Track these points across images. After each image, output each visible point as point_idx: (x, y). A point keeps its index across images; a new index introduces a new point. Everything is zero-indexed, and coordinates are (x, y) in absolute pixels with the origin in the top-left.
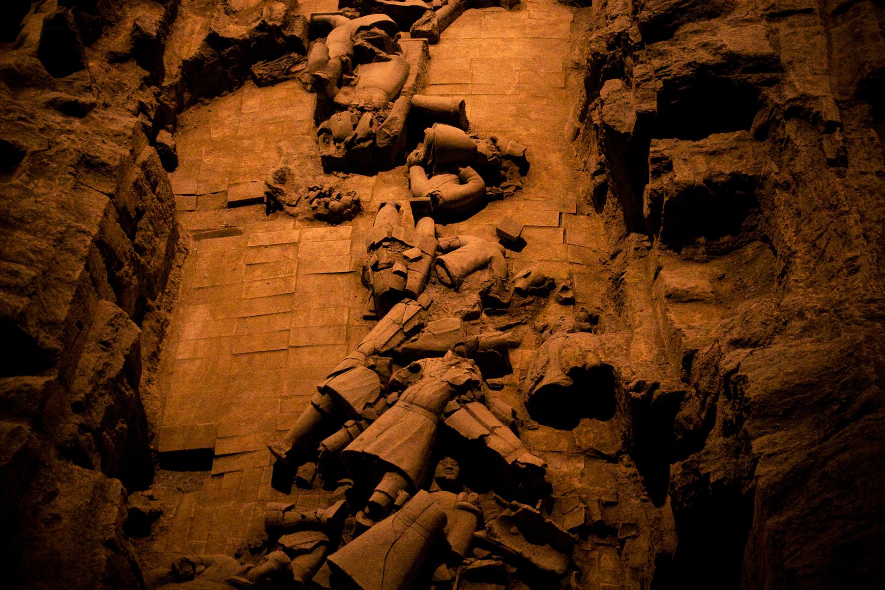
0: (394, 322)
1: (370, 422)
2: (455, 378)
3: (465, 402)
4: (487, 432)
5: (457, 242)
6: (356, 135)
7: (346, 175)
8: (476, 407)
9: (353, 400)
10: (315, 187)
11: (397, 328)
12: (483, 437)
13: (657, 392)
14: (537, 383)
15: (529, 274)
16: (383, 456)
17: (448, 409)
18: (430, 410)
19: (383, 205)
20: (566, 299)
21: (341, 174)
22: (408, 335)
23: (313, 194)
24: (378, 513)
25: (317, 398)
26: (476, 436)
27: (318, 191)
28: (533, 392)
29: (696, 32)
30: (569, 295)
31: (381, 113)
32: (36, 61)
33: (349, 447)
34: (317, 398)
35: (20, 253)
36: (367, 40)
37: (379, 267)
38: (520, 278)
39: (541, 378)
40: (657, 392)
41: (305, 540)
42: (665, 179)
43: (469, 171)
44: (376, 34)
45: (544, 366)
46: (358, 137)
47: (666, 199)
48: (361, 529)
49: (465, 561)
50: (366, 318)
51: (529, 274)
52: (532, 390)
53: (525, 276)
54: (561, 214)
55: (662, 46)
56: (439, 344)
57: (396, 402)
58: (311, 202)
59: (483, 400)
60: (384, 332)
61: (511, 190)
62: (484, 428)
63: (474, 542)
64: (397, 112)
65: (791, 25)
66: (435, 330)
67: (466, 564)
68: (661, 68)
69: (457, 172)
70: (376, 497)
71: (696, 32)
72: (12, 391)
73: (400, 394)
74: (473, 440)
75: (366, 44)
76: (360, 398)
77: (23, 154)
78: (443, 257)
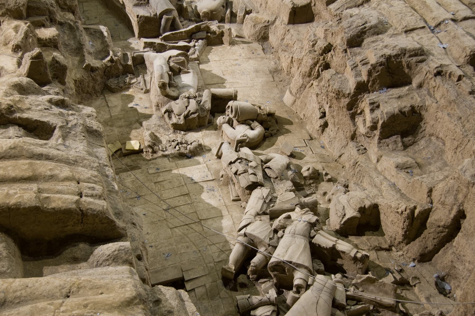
0: (259, 198)
1: (275, 247)
2: (310, 219)
3: (317, 230)
4: (335, 243)
5: (269, 158)
6: (190, 111)
7: (185, 133)
8: (321, 232)
9: (263, 237)
10: (174, 140)
11: (262, 201)
12: (334, 246)
13: (417, 212)
14: (343, 218)
15: (309, 169)
16: (294, 261)
17: (312, 235)
18: (304, 236)
19: (222, 144)
20: (329, 179)
21: (183, 132)
22: (268, 204)
23: (174, 144)
24: (299, 289)
25: (241, 239)
26: (331, 246)
27: (176, 142)
28: (342, 223)
29: (373, 42)
30: (329, 177)
31: (198, 99)
32: (29, 79)
33: (272, 260)
34: (241, 239)
35: (90, 178)
36: (176, 63)
37: (238, 173)
38: (305, 171)
39: (345, 215)
40: (417, 212)
41: (266, 311)
42: (378, 113)
43: (255, 124)
44: (180, 59)
45: (343, 209)
46: (191, 112)
47: (380, 122)
48: (295, 300)
49: (347, 308)
50: (234, 200)
51: (309, 169)
52: (341, 222)
53: (308, 169)
54: (304, 140)
55: (356, 50)
56: (287, 206)
57: (283, 235)
58: (175, 147)
59: (322, 229)
60: (257, 203)
61: (275, 131)
62: (332, 242)
63: (349, 298)
64: (206, 97)
65: (418, 35)
66: (283, 199)
67: (348, 309)
68: (363, 60)
69: (249, 125)
70: (297, 282)
71: (373, 42)
72: (115, 251)
73: (284, 232)
74: (330, 248)
75: (176, 65)
76: (266, 236)
77: (55, 128)
78: (268, 164)
